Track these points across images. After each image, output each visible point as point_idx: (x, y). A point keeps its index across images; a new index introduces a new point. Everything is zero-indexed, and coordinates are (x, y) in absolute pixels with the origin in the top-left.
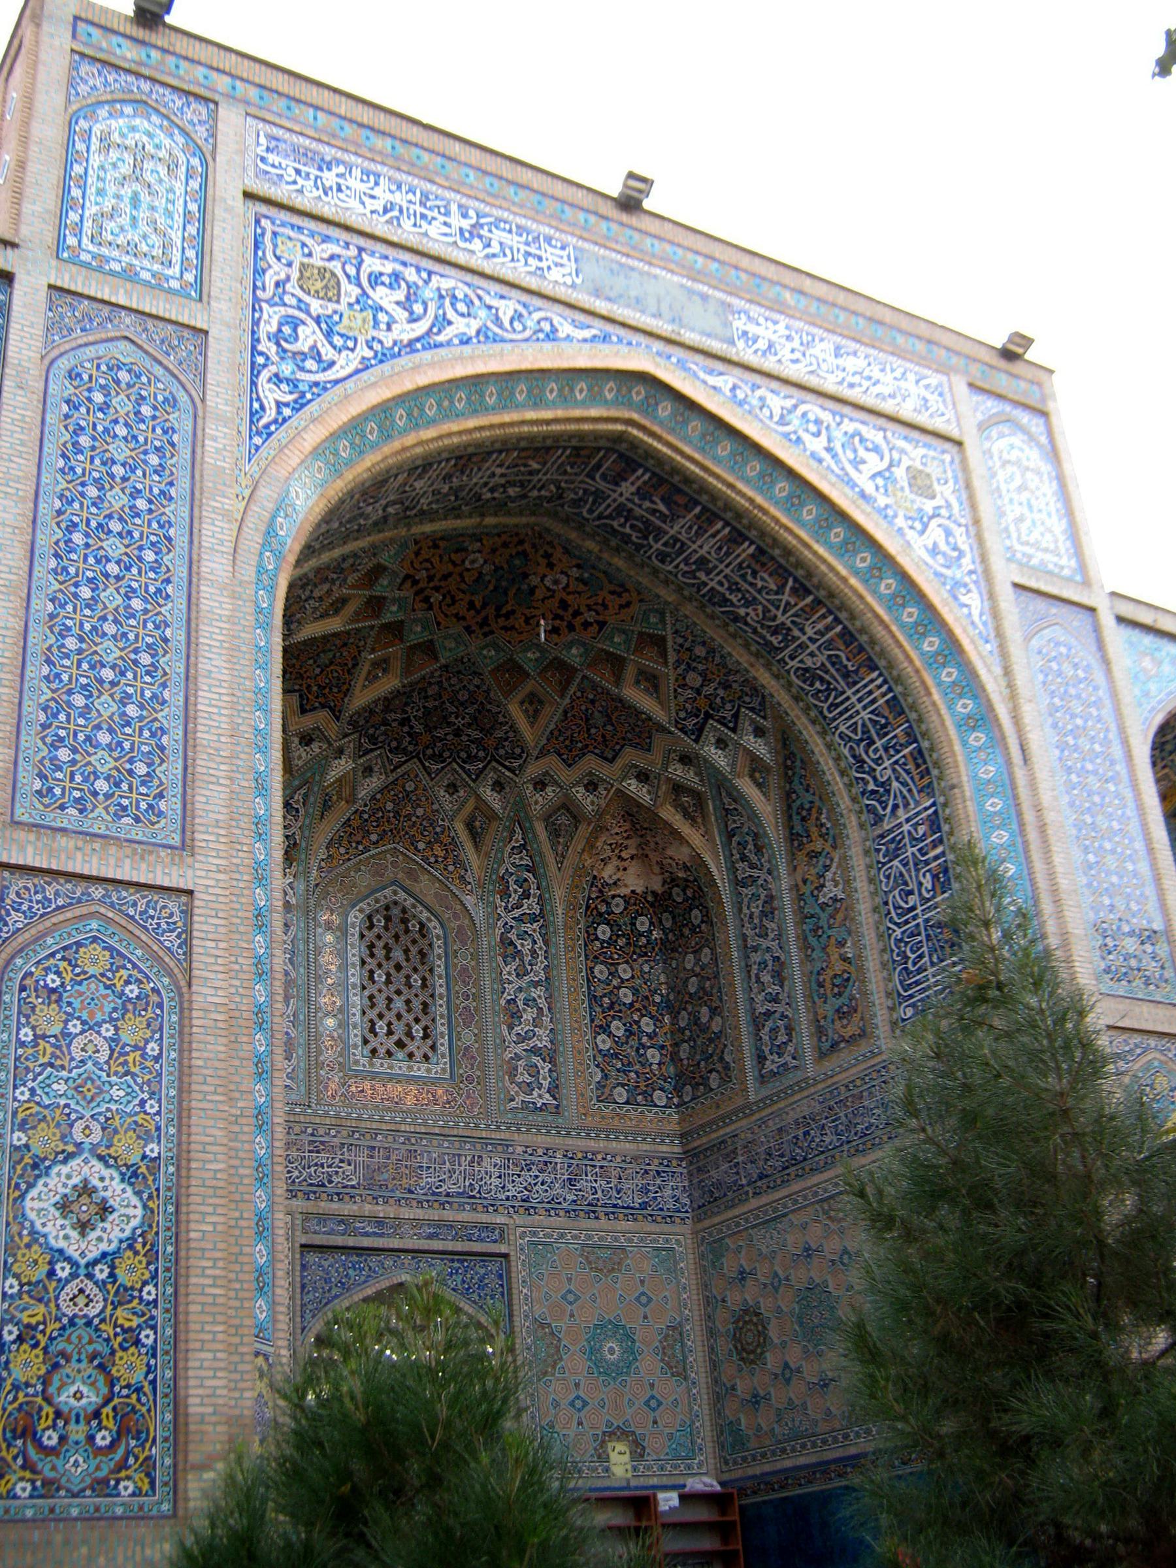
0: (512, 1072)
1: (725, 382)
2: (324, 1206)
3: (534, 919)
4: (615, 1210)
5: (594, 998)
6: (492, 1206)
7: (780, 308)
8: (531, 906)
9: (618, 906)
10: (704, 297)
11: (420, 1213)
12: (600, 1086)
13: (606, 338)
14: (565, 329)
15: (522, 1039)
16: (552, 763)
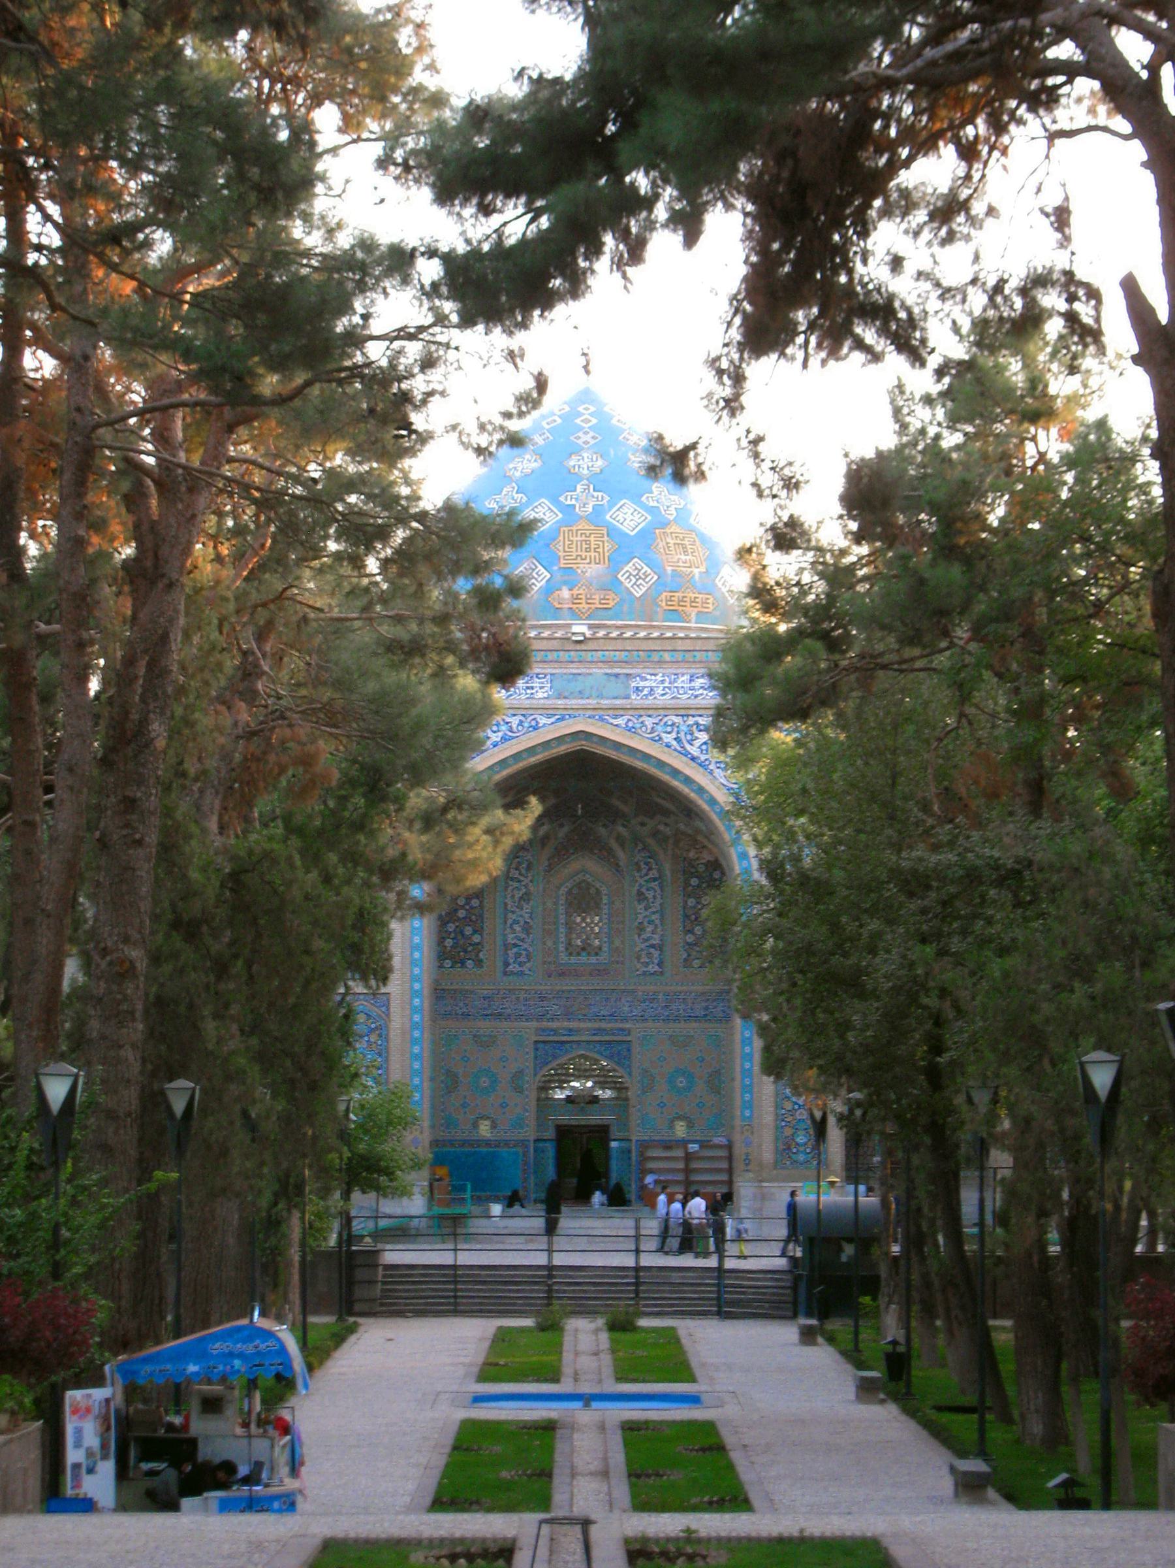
0: (638, 958)
1: (621, 721)
2: (545, 1024)
3: (654, 879)
4: (690, 1018)
5: (687, 916)
6: (625, 1020)
7: (661, 662)
8: (654, 873)
9: (701, 868)
10: (617, 675)
11: (590, 1025)
12: (686, 960)
13: (562, 719)
14: (543, 721)
15: (646, 940)
16: (641, 818)
